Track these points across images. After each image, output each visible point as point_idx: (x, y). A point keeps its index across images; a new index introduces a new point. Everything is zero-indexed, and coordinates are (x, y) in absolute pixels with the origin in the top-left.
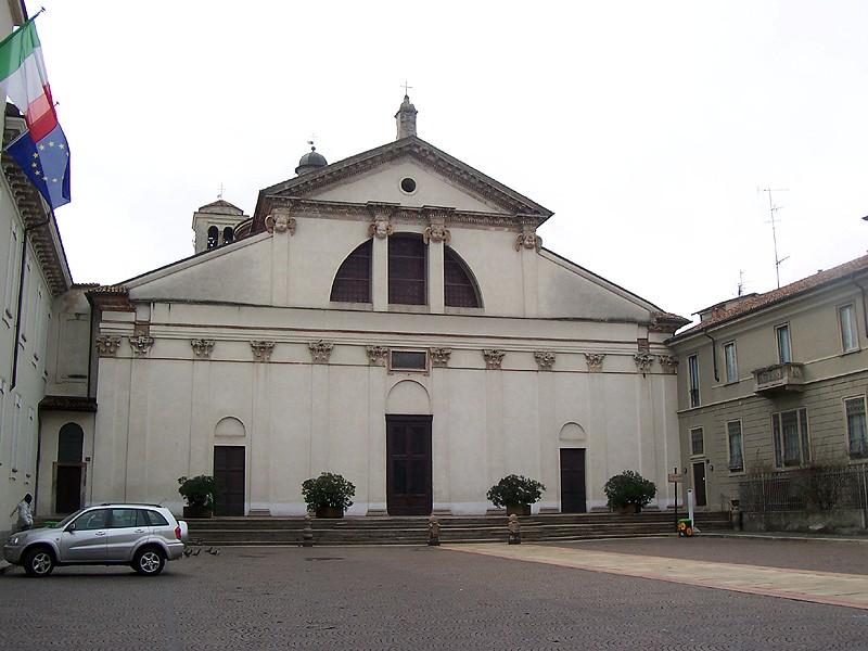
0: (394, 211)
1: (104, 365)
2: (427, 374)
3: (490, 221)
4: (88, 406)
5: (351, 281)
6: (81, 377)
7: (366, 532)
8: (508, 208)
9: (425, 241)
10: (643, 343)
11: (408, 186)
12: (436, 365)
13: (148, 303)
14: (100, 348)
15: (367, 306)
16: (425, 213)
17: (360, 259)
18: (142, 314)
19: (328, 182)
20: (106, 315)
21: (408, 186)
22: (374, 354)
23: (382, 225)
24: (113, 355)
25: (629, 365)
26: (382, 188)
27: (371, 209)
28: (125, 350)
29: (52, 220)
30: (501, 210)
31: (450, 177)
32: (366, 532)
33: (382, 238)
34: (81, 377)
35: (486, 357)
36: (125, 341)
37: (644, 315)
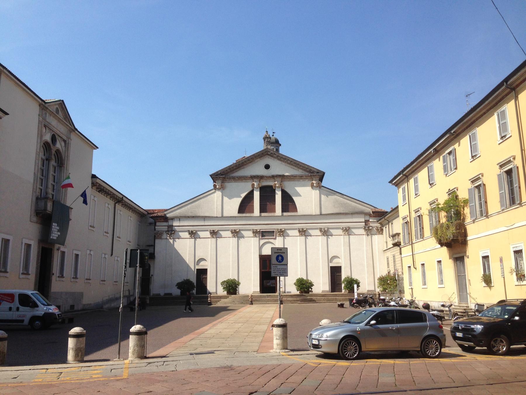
0: (261, 178)
1: (157, 241)
2: (275, 239)
3: (301, 177)
4: (152, 256)
5: (245, 206)
6: (152, 246)
7: (252, 300)
8: (307, 172)
9: (274, 188)
10: (366, 222)
11: (267, 167)
12: (280, 236)
13: (173, 219)
14: (157, 235)
15: (252, 215)
16: (273, 177)
17: (249, 198)
18: (170, 223)
19: (236, 169)
20: (158, 224)
21: (267, 167)
22: (255, 232)
23: (255, 184)
24: (161, 238)
25: (362, 231)
26: (258, 169)
27: (253, 178)
28: (165, 236)
29: (124, 198)
30: (307, 173)
31: (284, 162)
32: (252, 300)
33: (257, 188)
34: (152, 246)
35: (299, 231)
36: (165, 233)
37: (369, 210)
